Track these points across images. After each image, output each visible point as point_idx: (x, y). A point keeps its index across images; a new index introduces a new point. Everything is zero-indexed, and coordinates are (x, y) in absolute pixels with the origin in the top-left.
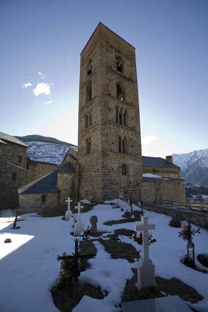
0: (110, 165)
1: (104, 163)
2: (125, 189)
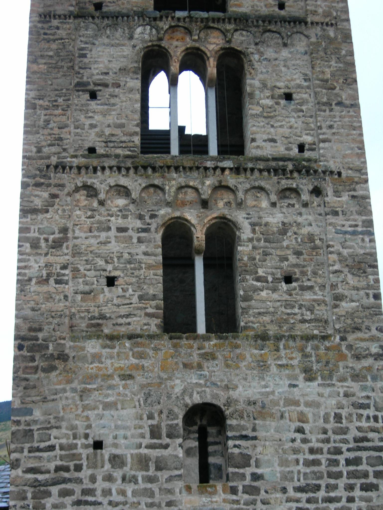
0: (80, 424)
1: (30, 412)
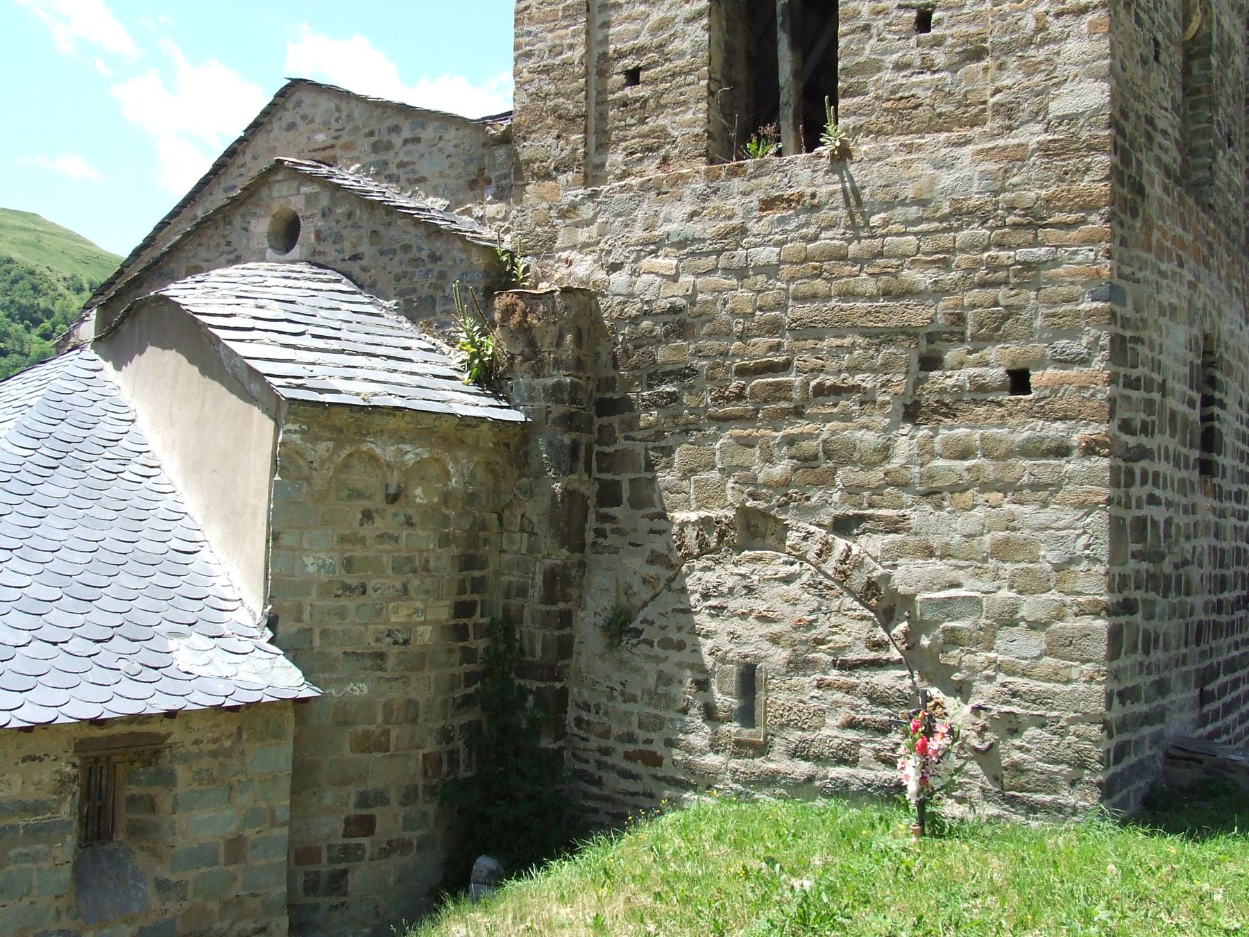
2: (1204, 646)
